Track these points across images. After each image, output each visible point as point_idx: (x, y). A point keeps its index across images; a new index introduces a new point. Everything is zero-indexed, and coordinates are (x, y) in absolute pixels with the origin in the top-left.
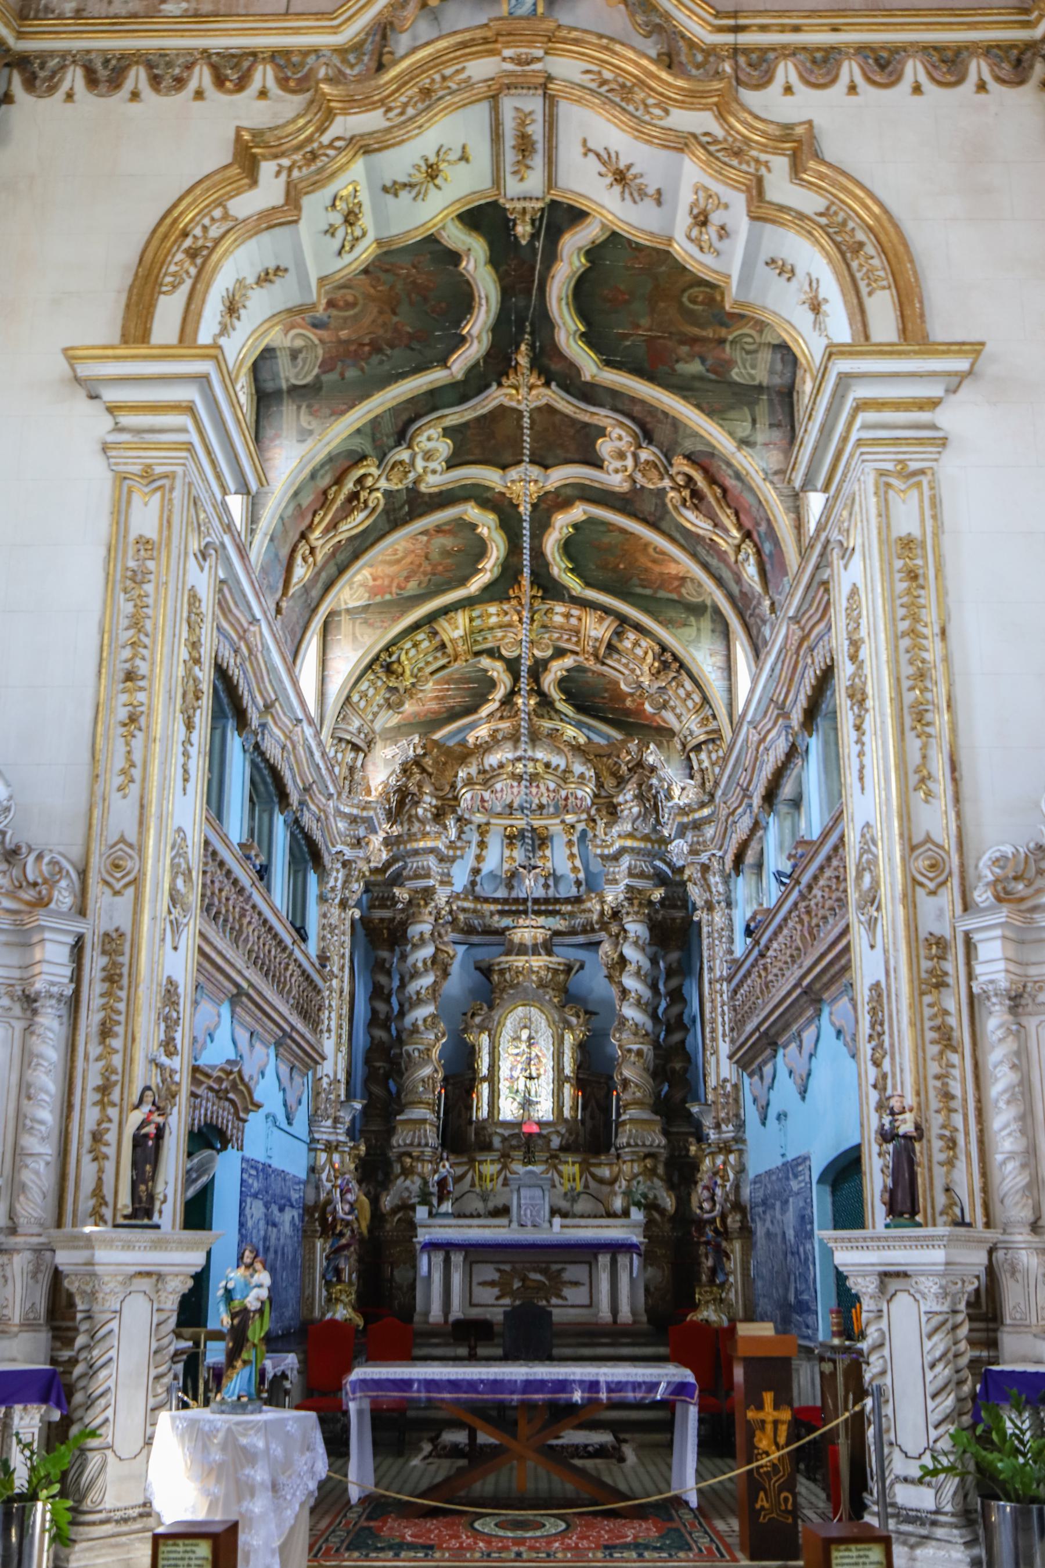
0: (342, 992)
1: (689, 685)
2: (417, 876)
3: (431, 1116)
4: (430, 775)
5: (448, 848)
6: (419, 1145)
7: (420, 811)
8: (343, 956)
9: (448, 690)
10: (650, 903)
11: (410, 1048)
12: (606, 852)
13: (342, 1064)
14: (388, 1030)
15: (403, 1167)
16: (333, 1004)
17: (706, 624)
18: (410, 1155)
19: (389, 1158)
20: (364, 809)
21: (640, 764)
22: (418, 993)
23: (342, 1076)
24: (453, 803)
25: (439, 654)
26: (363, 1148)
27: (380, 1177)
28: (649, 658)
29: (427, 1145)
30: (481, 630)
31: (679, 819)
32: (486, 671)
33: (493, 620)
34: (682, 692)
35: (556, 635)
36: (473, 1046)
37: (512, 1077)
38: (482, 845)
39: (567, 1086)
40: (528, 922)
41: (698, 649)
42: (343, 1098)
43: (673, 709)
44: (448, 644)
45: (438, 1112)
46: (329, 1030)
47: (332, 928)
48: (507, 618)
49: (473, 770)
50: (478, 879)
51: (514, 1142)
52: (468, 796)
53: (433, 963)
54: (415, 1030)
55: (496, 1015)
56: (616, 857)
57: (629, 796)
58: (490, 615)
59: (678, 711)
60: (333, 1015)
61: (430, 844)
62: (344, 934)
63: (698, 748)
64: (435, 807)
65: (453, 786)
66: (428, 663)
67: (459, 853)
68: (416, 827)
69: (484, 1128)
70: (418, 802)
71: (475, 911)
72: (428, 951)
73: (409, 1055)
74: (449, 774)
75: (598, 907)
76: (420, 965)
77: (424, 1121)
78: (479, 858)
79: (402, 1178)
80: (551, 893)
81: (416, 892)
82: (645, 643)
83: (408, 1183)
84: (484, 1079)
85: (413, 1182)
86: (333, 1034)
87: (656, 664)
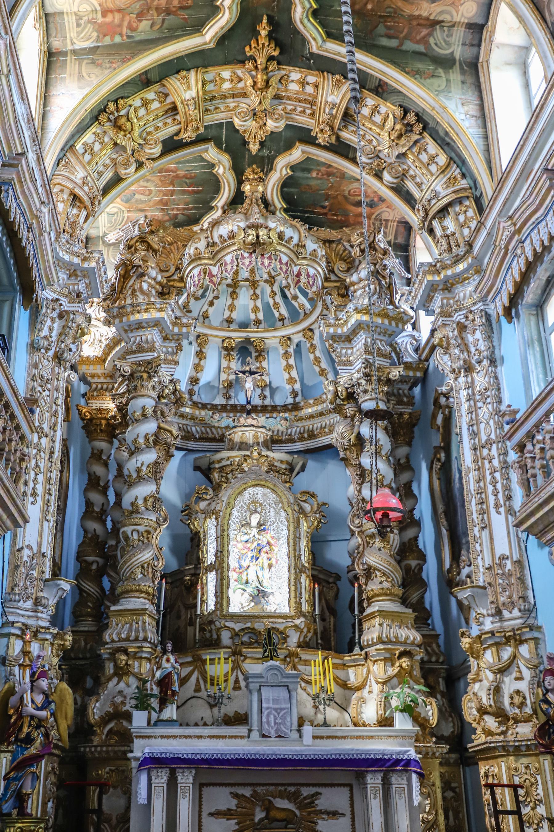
0: (52, 453)
1: (432, 147)
2: (140, 350)
3: (151, 608)
4: (155, 251)
5: (174, 324)
6: (136, 640)
7: (145, 286)
8: (55, 414)
9: (172, 193)
10: (389, 382)
11: (128, 529)
12: (339, 331)
13: (48, 538)
14: (104, 523)
15: (116, 666)
16: (41, 465)
17: (455, 76)
18: (125, 652)
19: (100, 656)
20: (85, 259)
21: (372, 246)
22: (138, 470)
23: (47, 549)
24: (178, 284)
25: (169, 121)
26: (69, 638)
27: (89, 683)
28: (390, 123)
29: (145, 639)
30: (213, 98)
31: (430, 278)
32: (213, 166)
33: (227, 86)
34: (424, 157)
35: (289, 108)
36: (197, 533)
37: (241, 567)
38: (200, 355)
39: (303, 576)
40: (250, 421)
41: (449, 99)
42: (47, 576)
43: (413, 178)
44: (180, 106)
45: (158, 606)
46: (34, 494)
47: (45, 382)
48: (241, 85)
49: (202, 245)
50: (196, 388)
51: (245, 639)
52: (196, 272)
53: (156, 442)
54: (135, 510)
55: (225, 495)
56: (349, 339)
57: (363, 273)
58: (223, 80)
59: (418, 180)
60: (40, 477)
61: (156, 315)
62: (57, 390)
63: (443, 211)
64: (160, 283)
65: (178, 269)
66: (157, 128)
67: (184, 330)
68: (141, 298)
69: (211, 622)
70: (142, 275)
71: (193, 418)
72: (150, 427)
73: (127, 538)
74: (174, 256)
75: (331, 388)
76: (141, 441)
77: (143, 611)
78: (197, 367)
79: (115, 680)
80: (268, 402)
81: (140, 365)
82: (386, 108)
83: (122, 685)
84: (211, 568)
85: (128, 685)
86: (39, 499)
87: (398, 127)
